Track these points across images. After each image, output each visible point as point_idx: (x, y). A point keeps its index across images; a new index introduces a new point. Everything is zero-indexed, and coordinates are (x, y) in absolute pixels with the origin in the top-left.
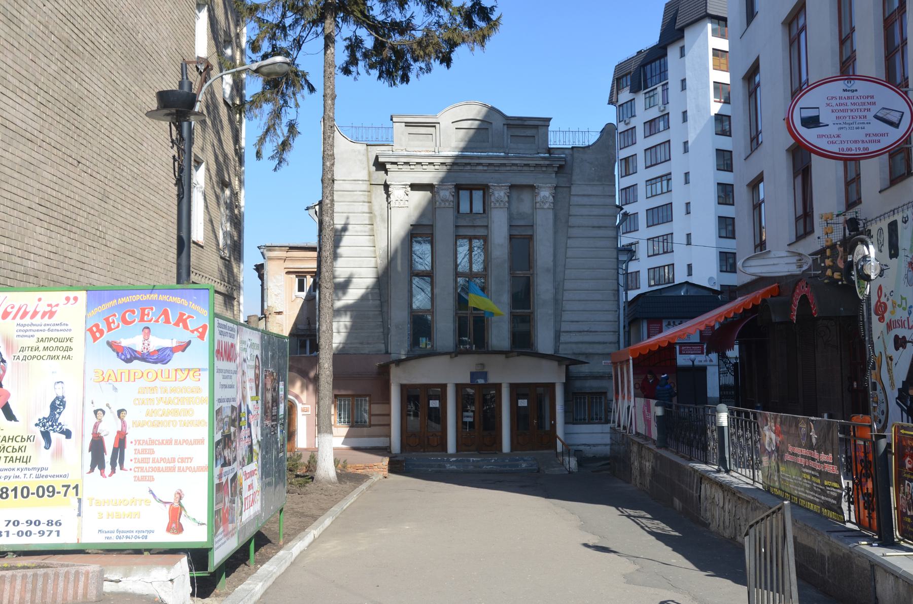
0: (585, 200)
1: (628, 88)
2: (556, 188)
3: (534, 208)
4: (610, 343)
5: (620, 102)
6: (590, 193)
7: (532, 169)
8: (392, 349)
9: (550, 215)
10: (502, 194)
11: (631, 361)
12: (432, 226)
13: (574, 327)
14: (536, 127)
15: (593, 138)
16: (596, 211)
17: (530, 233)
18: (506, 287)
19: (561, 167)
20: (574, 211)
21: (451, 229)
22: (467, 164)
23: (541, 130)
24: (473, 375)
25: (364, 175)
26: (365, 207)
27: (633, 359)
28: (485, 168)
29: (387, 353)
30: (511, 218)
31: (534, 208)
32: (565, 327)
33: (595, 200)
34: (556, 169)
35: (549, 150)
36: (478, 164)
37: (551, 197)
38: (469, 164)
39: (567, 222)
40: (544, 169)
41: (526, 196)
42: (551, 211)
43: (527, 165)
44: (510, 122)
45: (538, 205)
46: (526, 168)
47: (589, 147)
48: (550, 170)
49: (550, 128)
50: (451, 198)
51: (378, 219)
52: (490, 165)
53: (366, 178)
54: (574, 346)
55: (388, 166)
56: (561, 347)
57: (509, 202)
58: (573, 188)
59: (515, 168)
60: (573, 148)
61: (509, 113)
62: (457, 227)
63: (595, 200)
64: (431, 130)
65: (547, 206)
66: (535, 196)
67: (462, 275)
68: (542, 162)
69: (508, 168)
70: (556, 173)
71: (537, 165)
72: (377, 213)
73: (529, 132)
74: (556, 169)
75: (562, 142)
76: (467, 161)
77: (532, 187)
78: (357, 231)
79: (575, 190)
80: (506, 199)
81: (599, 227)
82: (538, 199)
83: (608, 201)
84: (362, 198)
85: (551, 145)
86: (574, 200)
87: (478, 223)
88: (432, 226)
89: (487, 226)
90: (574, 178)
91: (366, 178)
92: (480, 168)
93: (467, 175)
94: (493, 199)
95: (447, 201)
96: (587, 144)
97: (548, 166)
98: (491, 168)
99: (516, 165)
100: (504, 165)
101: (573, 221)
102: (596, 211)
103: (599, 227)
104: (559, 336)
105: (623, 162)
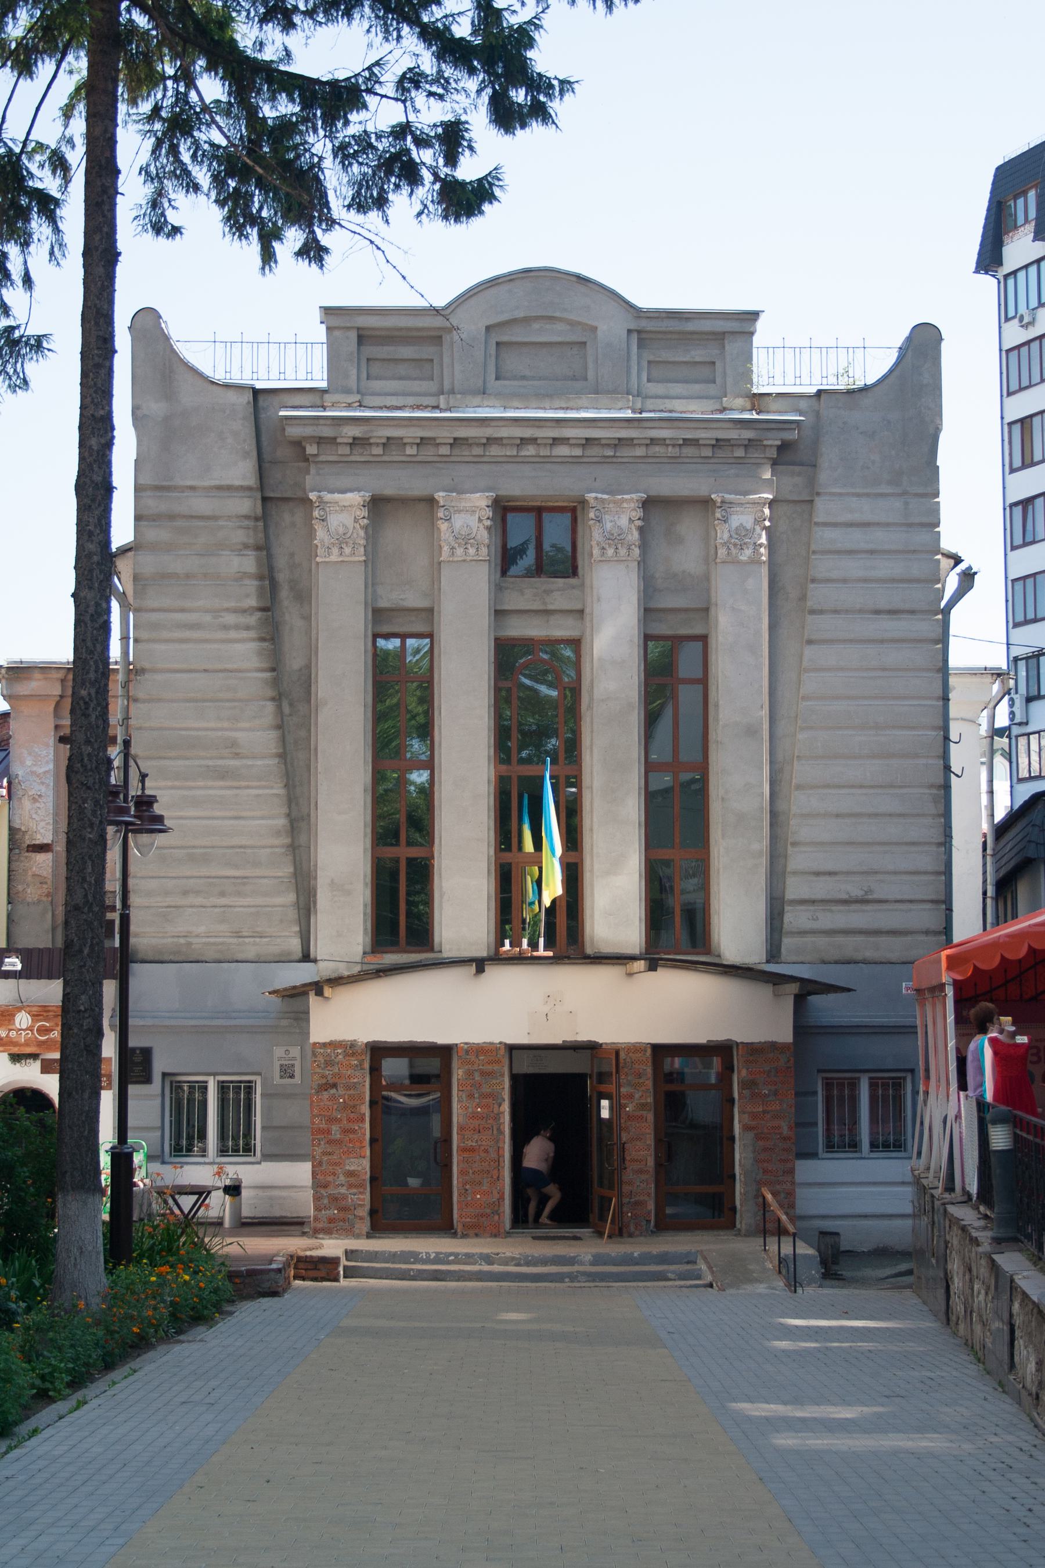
0: (856, 538)
1: (1030, 227)
4: (927, 933)
5: (1008, 266)
6: (868, 517)
8: (321, 948)
11: (950, 991)
12: (431, 610)
13: (822, 889)
14: (720, 337)
15: (873, 366)
16: (885, 568)
17: (698, 630)
18: (634, 779)
19: (784, 447)
20: (823, 566)
21: (483, 619)
22: (524, 441)
23: (732, 347)
25: (241, 471)
26: (249, 563)
27: (956, 984)
29: (306, 957)
30: (648, 588)
32: (795, 888)
33: (880, 538)
35: (758, 401)
36: (556, 441)
38: (533, 441)
39: (803, 598)
41: (688, 526)
43: (694, 442)
44: (644, 324)
46: (689, 451)
47: (865, 389)
48: (755, 454)
49: (757, 340)
51: (284, 593)
52: (589, 442)
54: (822, 941)
55: (311, 449)
56: (787, 942)
57: (644, 546)
58: (820, 504)
60: (820, 392)
61: (647, 297)
63: (880, 538)
64: (427, 351)
68: (733, 434)
69: (640, 452)
70: (775, 463)
71: (719, 444)
72: (282, 577)
74: (773, 453)
75: (790, 379)
76: (528, 433)
77: (705, 504)
78: (226, 627)
79: (823, 509)
81: (892, 612)
82: (723, 534)
83: (921, 537)
85: (761, 385)
86: (825, 537)
87: (558, 601)
88: (431, 610)
89: (581, 612)
90: (824, 476)
91: (252, 481)
92: (563, 451)
96: (860, 383)
97: (749, 444)
100: (629, 442)
101: (818, 595)
102: (885, 568)
103: (892, 612)
104: (781, 914)
105: (1017, 429)
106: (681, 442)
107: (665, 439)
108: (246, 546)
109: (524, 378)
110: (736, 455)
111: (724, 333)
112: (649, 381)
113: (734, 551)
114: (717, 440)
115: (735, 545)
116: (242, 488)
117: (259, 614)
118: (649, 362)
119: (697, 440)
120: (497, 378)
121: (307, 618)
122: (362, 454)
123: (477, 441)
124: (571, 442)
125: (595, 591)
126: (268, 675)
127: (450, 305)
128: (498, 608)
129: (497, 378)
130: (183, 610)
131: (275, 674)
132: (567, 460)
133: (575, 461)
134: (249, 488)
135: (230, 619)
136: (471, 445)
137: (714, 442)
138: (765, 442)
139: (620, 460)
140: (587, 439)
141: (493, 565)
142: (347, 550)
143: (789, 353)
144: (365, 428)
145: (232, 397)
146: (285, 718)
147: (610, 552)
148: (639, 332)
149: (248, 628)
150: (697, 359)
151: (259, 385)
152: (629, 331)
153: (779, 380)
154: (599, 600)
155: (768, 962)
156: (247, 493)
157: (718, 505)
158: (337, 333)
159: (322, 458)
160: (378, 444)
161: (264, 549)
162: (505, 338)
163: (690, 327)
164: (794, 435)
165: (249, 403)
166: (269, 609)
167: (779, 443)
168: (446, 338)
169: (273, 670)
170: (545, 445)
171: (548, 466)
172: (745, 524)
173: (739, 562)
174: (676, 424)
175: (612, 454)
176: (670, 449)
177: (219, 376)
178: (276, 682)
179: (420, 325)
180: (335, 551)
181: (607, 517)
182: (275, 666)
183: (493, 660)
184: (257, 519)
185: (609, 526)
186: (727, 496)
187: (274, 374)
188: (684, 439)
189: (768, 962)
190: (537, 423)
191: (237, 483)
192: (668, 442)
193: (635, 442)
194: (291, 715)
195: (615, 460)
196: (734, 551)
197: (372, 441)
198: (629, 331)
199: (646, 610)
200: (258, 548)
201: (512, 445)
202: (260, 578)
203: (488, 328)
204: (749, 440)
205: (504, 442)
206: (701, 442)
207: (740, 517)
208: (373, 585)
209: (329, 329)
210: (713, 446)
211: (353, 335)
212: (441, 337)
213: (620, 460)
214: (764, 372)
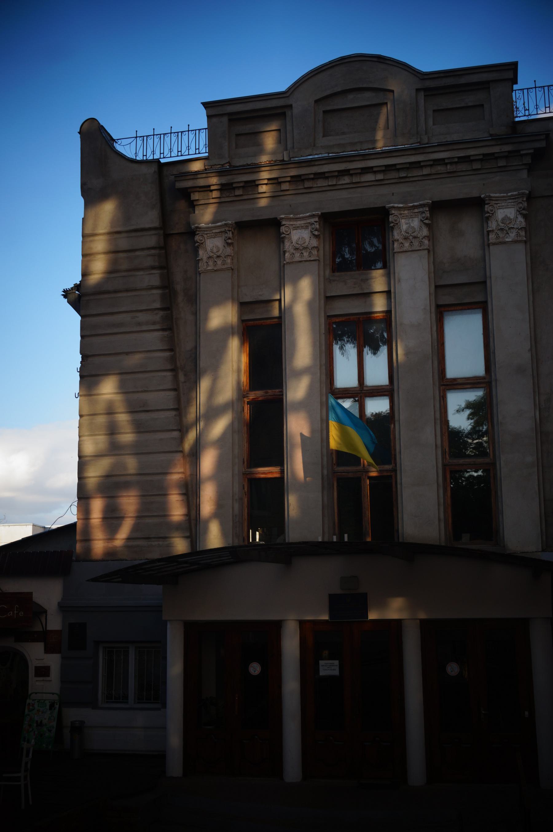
2: (530, 198)
3: (486, 245)
7: (477, 166)
9: (520, 254)
10: (416, 223)
14: (484, 86)
19: (538, 156)
24: (335, 602)
26: (154, 278)
28: (380, 177)
31: (486, 245)
34: (528, 160)
37: (520, 219)
40: (502, 163)
42: (521, 248)
45: (492, 236)
46: (463, 167)
50: (314, 242)
51: (180, 298)
52: (388, 168)
53: (156, 224)
55: (195, 196)
57: (432, 238)
59: (440, 169)
62: (329, 299)
65: (512, 236)
66: (485, 219)
67: (346, 393)
69: (426, 171)
71: (486, 158)
72: (179, 287)
73: (470, 99)
74: (528, 160)
78: (139, 324)
80: (425, 232)
82: (493, 225)
84: (149, 262)
91: (156, 224)
92: (370, 177)
93: (344, 194)
94: (396, 235)
95: (305, 248)
98: (393, 175)
99: (441, 162)
106: (456, 160)
107: (443, 159)
108: (153, 268)
109: (343, 133)
110: (500, 165)
111: (488, 82)
112: (434, 124)
113: (501, 235)
114: (484, 155)
115: (502, 230)
116: (150, 229)
117: (161, 313)
118: (434, 111)
119: (469, 157)
120: (324, 136)
121: (195, 314)
122: (228, 197)
123: (307, 177)
124: (375, 169)
125: (396, 275)
126: (168, 354)
127: (289, 89)
128: (328, 295)
129: (324, 136)
130: (112, 314)
131: (172, 353)
132: (373, 183)
133: (379, 183)
134: (155, 229)
135: (142, 317)
136: (303, 180)
137: (481, 157)
138: (522, 152)
139: (411, 179)
140: (386, 166)
141: (322, 263)
142: (219, 262)
143: (540, 94)
144: (229, 177)
145: (144, 169)
146: (181, 384)
147: (407, 245)
148: (425, 90)
149: (154, 323)
150: (470, 104)
151: (163, 161)
152: (418, 90)
153: (532, 110)
154: (399, 281)
155: (543, 550)
156: (153, 232)
157: (487, 202)
158: (214, 120)
159: (202, 202)
160: (238, 188)
161: (165, 268)
162: (329, 108)
163: (463, 80)
164: (543, 144)
165: (155, 172)
166: (168, 307)
167: (532, 151)
168: (288, 113)
169: (171, 350)
170: (356, 174)
171: (360, 190)
172: (509, 215)
173: (505, 243)
174: (451, 147)
175: (405, 175)
176: (449, 167)
177: (140, 158)
178: (173, 359)
179: (270, 106)
180: (211, 263)
181: (403, 221)
182: (172, 347)
183: (323, 331)
184: (160, 248)
185: (404, 227)
186: (492, 195)
187: (174, 153)
188: (459, 158)
189: (543, 550)
190: (348, 159)
191: (147, 226)
192: (446, 161)
193: (422, 164)
194: (185, 382)
195: (407, 180)
196: (501, 235)
197: (234, 185)
198: (418, 90)
199: (437, 287)
200: (161, 268)
201: (332, 177)
202: (162, 287)
203: (316, 101)
204: (509, 152)
205: (327, 175)
206: (472, 158)
207: (505, 210)
208: (239, 287)
209: (209, 117)
210: (481, 160)
211: (225, 119)
212: (284, 114)
213: (411, 179)
214: (521, 108)
